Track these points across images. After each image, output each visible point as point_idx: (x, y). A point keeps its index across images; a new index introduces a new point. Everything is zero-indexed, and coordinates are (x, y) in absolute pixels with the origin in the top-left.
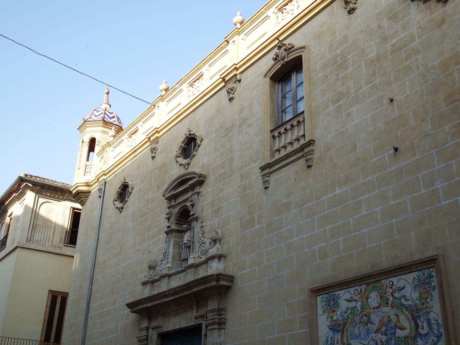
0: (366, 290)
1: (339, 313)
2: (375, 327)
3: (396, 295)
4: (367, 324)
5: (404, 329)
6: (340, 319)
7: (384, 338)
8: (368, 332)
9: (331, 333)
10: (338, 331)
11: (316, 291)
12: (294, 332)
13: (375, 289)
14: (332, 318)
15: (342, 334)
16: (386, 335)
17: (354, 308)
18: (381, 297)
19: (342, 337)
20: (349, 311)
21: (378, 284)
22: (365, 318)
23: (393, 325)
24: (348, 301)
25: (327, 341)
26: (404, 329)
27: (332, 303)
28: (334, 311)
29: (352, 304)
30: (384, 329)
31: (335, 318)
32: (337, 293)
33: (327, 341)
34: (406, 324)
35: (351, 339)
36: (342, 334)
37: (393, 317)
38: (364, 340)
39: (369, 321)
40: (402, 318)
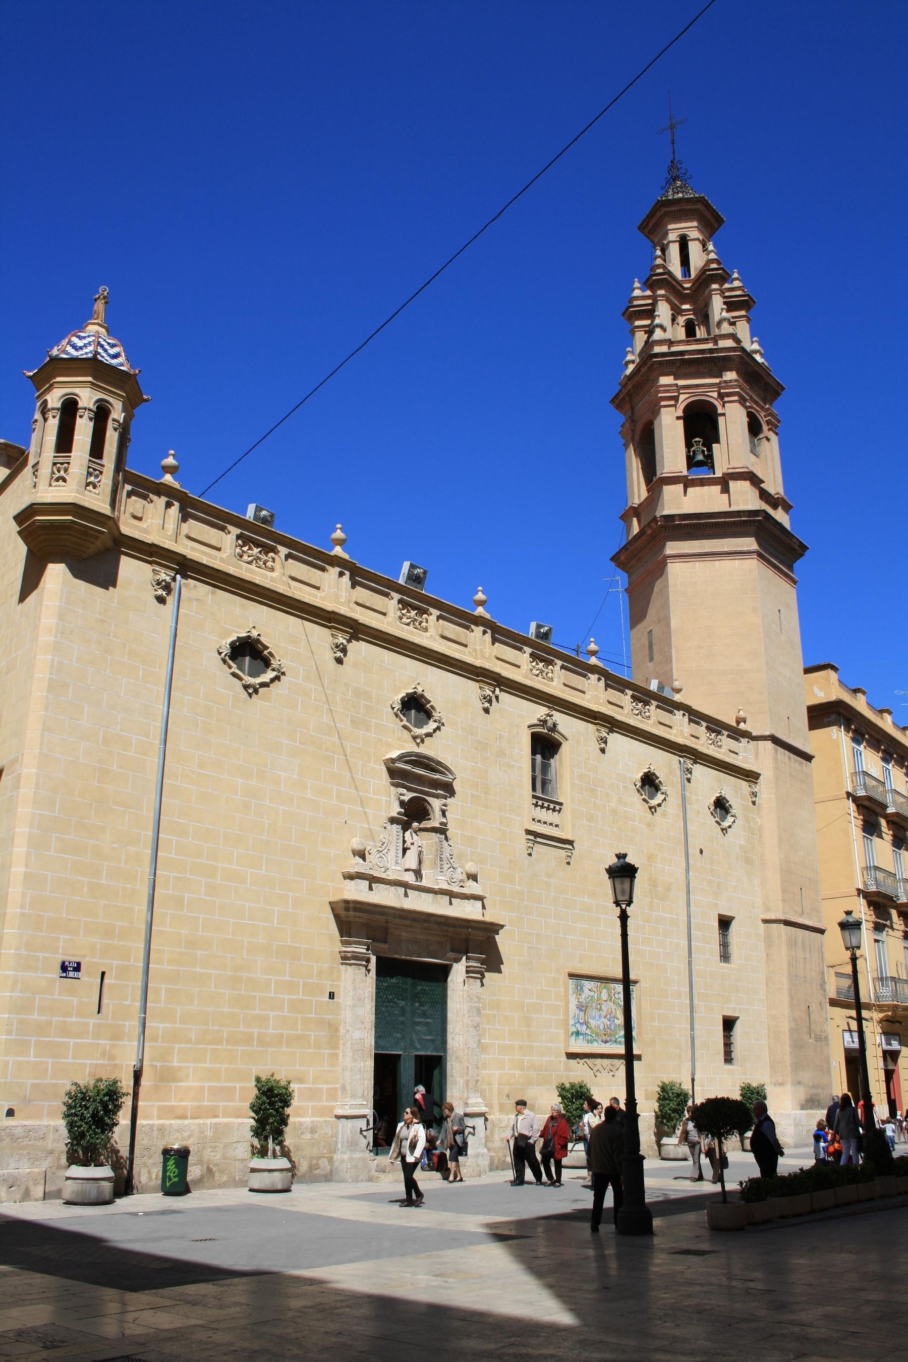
0: (600, 986)
1: (583, 996)
2: (604, 1014)
3: (616, 996)
4: (600, 1010)
5: (618, 1019)
6: (584, 1002)
7: (608, 1023)
8: (600, 1016)
9: (577, 1011)
10: (582, 1011)
11: (572, 975)
12: (550, 1002)
13: (605, 987)
14: (579, 999)
15: (585, 1014)
16: (609, 1021)
17: (592, 997)
18: (609, 995)
19: (585, 1016)
20: (590, 998)
21: (607, 985)
22: (599, 1006)
23: (613, 1015)
24: (590, 990)
25: (575, 1016)
26: (618, 1019)
27: (579, 988)
28: (580, 995)
29: (592, 994)
30: (608, 1016)
31: (580, 1000)
32: (583, 982)
33: (575, 1016)
34: (620, 1017)
35: (590, 1018)
36: (585, 1014)
37: (613, 1010)
38: (598, 1021)
39: (600, 1009)
40: (618, 1012)
